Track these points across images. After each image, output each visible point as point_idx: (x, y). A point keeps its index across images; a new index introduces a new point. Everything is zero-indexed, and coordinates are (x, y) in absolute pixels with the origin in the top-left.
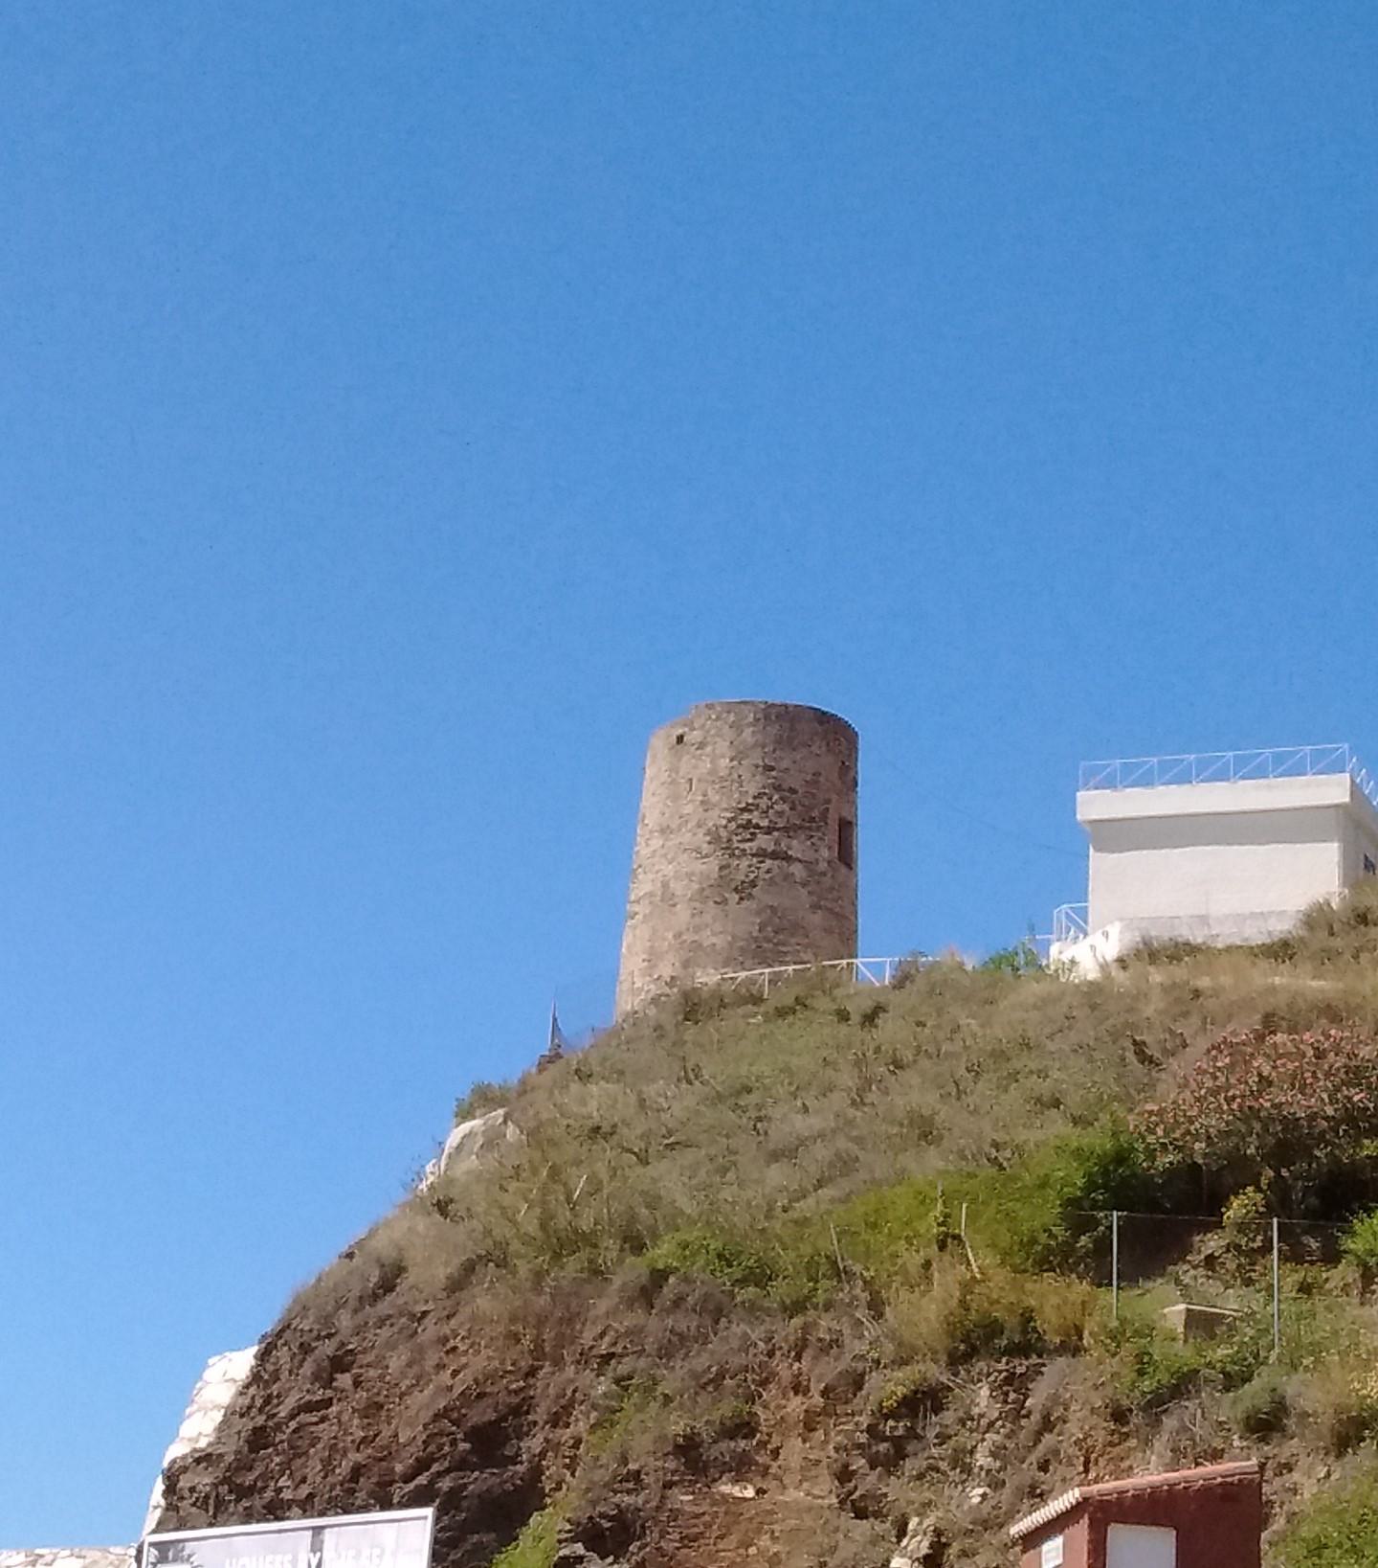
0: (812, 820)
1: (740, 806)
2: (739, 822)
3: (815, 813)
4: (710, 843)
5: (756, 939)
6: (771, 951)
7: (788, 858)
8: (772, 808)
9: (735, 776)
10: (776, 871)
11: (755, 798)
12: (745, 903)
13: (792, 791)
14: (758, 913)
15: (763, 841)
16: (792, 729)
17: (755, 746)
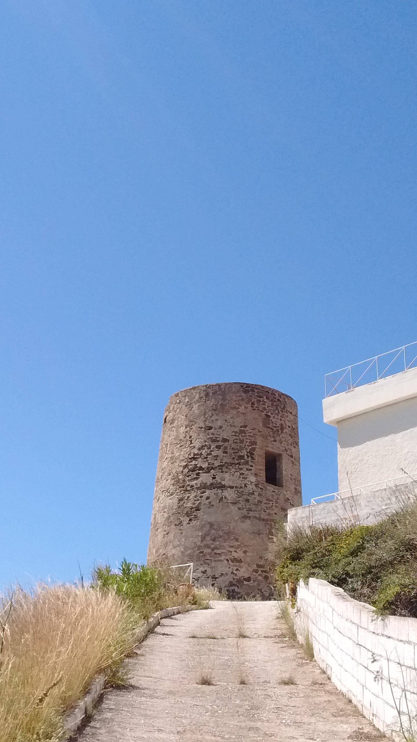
0: (242, 457)
1: (190, 457)
2: (190, 467)
3: (244, 453)
4: (173, 485)
5: (199, 547)
6: (210, 554)
7: (222, 487)
8: (210, 454)
9: (188, 438)
10: (213, 497)
11: (199, 449)
12: (194, 523)
13: (225, 440)
14: (202, 527)
15: (205, 478)
16: (224, 399)
17: (199, 416)
